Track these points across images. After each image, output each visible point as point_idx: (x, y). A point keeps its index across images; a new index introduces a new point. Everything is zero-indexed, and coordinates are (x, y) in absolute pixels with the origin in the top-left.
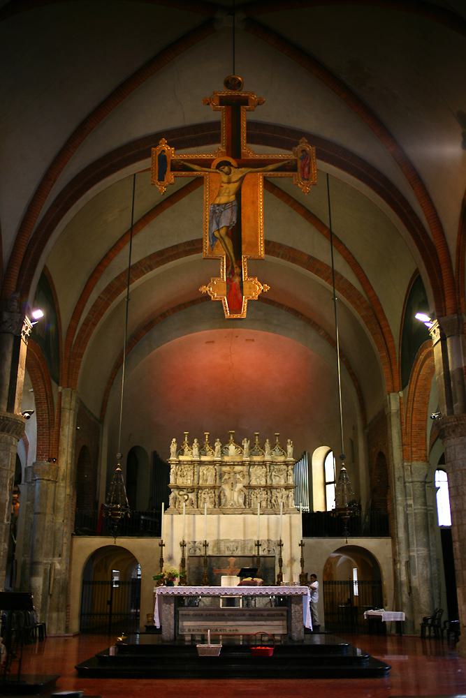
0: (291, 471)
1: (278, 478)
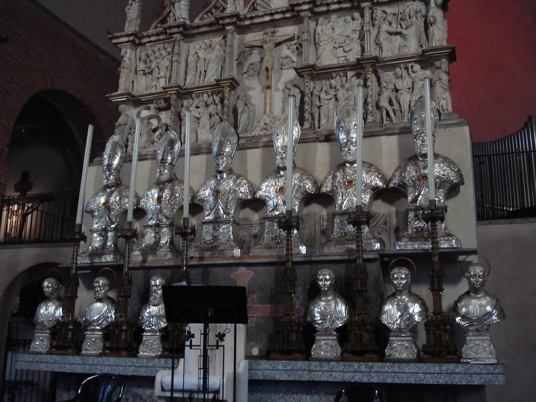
0: (436, 13)
1: (398, 40)
